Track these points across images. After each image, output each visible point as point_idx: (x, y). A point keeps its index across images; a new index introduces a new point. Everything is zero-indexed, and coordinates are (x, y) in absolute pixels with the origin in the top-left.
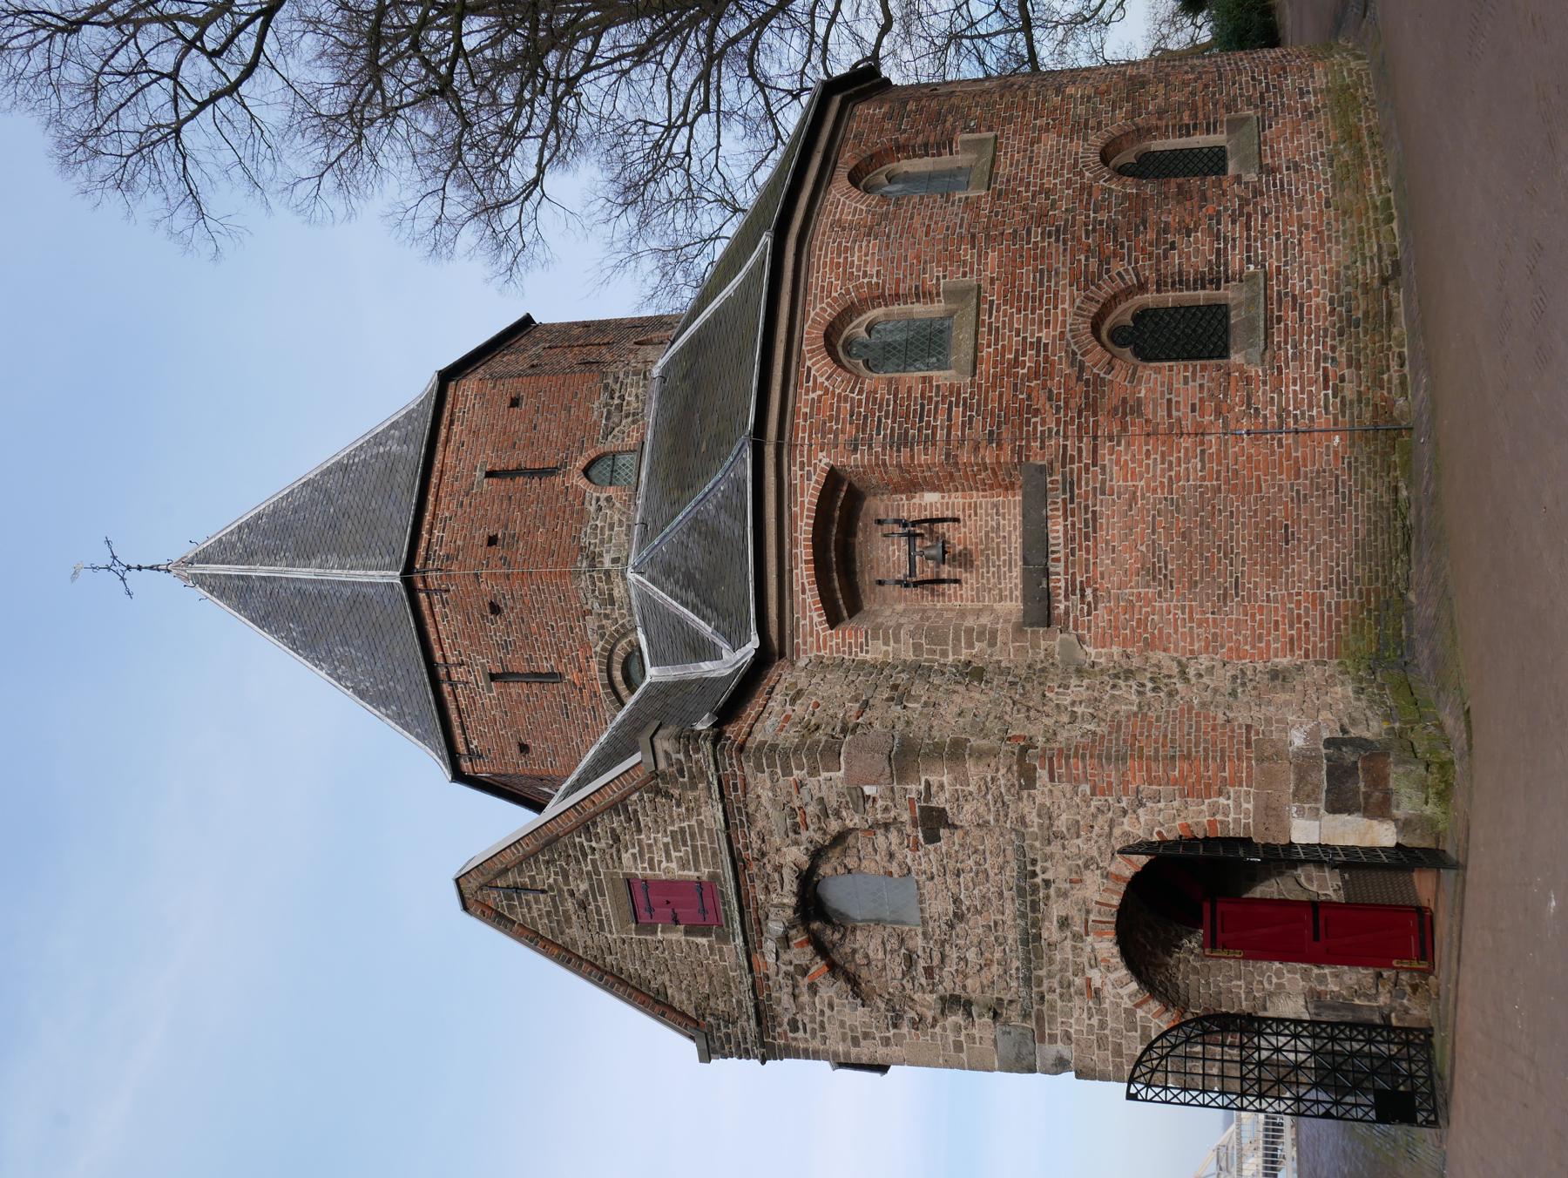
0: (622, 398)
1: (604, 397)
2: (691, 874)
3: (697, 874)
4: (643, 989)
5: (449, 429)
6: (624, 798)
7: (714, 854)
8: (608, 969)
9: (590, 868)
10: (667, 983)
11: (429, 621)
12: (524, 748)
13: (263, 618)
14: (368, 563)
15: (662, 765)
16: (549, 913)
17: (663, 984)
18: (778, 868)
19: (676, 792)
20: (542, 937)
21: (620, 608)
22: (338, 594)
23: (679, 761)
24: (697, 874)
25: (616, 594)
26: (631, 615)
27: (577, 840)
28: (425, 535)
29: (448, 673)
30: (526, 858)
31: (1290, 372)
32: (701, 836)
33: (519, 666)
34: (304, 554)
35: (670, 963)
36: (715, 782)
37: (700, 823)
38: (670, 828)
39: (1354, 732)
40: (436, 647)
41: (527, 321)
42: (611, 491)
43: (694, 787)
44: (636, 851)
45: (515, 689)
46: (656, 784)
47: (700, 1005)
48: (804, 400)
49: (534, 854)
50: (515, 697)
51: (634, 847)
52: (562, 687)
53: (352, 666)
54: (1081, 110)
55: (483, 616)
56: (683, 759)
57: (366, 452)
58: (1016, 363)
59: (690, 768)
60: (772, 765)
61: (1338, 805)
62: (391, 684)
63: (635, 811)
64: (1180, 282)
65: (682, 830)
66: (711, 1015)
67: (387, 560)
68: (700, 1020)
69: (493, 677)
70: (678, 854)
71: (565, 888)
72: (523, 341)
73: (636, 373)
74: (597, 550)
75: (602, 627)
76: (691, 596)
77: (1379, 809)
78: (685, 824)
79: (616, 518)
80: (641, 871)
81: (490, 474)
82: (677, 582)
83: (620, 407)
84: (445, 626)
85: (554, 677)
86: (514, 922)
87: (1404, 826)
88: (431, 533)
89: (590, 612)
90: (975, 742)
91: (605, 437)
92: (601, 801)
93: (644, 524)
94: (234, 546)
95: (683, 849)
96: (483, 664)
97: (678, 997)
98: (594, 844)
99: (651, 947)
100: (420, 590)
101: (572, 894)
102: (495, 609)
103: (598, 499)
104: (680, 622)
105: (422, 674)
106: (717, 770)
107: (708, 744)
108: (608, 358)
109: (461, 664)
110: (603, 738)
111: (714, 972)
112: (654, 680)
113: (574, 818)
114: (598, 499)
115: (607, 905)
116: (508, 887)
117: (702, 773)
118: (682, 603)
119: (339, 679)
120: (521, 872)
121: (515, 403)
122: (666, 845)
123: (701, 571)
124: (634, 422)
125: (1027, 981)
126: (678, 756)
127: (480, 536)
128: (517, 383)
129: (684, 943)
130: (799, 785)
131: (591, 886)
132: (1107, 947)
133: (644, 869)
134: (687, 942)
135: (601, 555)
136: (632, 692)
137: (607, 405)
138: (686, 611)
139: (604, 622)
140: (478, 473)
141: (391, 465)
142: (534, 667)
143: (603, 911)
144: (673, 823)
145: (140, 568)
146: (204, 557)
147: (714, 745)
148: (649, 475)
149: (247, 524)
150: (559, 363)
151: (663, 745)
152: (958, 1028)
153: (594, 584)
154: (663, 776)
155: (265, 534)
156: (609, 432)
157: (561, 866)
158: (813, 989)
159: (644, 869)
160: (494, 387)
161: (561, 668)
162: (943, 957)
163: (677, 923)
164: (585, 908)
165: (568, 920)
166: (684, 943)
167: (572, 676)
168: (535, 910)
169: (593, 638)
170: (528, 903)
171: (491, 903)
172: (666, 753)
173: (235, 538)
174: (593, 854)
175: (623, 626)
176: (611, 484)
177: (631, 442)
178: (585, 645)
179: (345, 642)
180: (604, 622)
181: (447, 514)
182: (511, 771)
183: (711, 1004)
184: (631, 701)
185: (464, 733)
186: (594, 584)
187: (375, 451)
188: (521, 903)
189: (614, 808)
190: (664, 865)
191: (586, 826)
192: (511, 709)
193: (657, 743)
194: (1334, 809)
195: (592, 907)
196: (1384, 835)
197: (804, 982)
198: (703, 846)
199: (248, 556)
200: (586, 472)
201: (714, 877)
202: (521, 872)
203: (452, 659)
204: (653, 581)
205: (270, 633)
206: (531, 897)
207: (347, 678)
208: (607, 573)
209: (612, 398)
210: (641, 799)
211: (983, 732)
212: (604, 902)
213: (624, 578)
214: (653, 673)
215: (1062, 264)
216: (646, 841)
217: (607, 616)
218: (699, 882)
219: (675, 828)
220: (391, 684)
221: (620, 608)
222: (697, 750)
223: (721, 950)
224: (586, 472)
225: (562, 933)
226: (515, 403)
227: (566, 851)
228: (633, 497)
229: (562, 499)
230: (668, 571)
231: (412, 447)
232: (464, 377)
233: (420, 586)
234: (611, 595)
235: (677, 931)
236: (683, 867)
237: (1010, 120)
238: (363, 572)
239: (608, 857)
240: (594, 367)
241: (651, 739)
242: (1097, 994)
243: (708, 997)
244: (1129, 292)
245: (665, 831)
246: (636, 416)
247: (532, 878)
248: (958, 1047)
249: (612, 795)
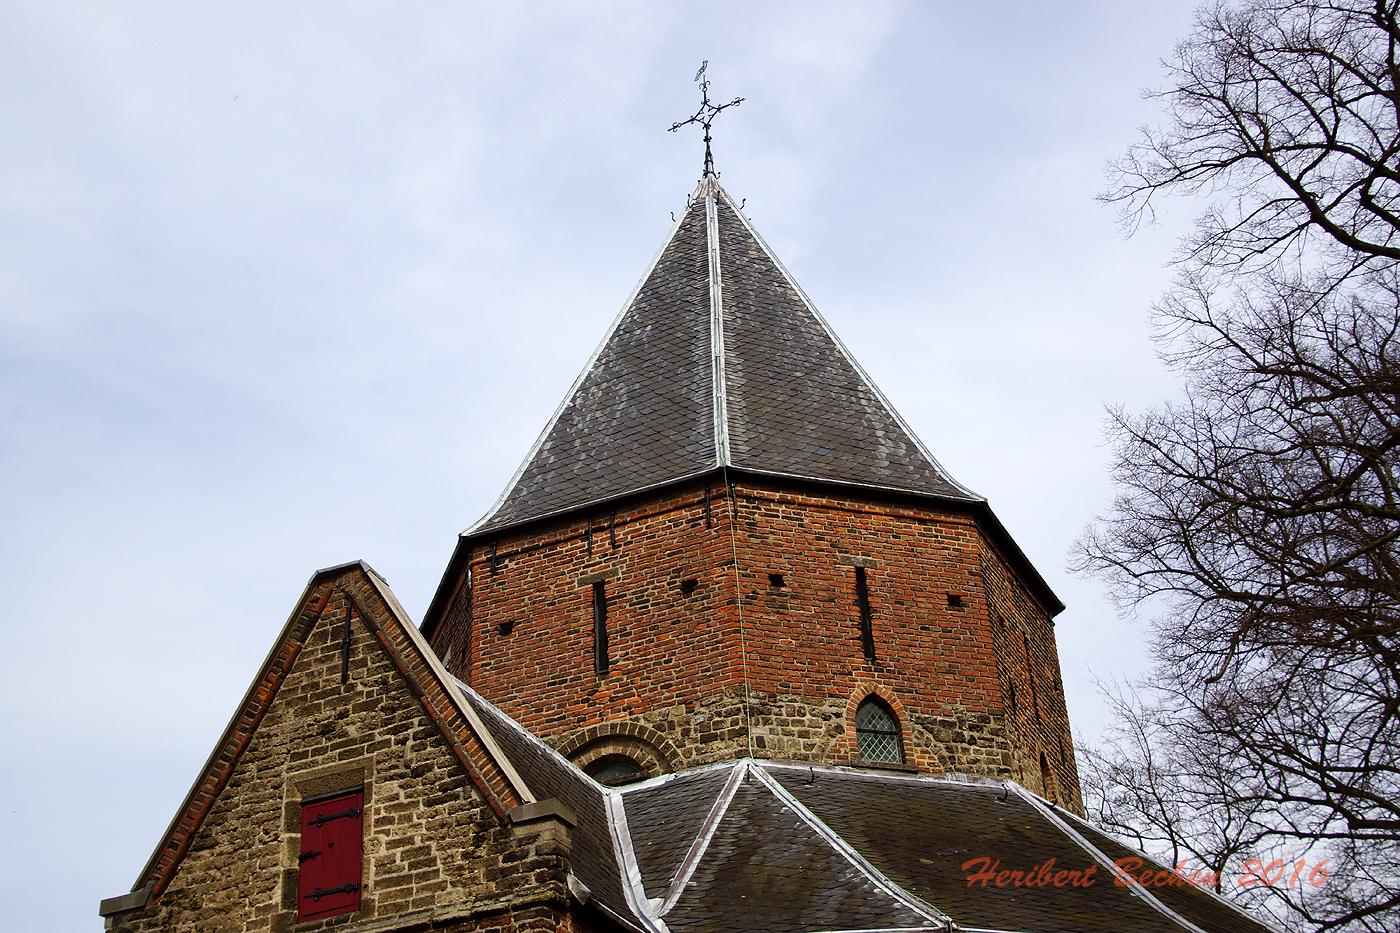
0: (972, 741)
1: (971, 718)
2: (371, 876)
3: (371, 884)
4: (210, 816)
5: (913, 519)
6: (472, 782)
7: (399, 907)
8: (238, 768)
9: (378, 738)
10: (217, 849)
12: (506, 628)
13: (654, 291)
14: (739, 423)
15: (520, 832)
16: (316, 685)
17: (217, 844)
19: (483, 852)
20: (283, 677)
21: (697, 749)
22: (694, 387)
23: (526, 854)
24: (371, 884)
25: (717, 744)
26: (690, 766)
27: (416, 721)
28: (777, 496)
29: (602, 529)
30: (388, 654)
32: (423, 889)
33: (615, 619)
34: (742, 342)
35: (247, 852)
36: (499, 906)
37: (441, 886)
38: (433, 844)
41: (1056, 607)
42: (851, 732)
43: (491, 876)
44: (403, 800)
45: (585, 615)
46: (494, 824)
47: (185, 896)
49: (395, 665)
50: (574, 614)
51: (407, 797)
52: (589, 674)
53: (602, 405)
55: (678, 571)
56: (528, 860)
57: (876, 414)
59: (515, 869)
62: (583, 456)
63: (456, 797)
65: (435, 859)
66: (171, 914)
67: (744, 448)
68: (163, 898)
69: (599, 587)
70: (398, 856)
71: (350, 707)
72: (1030, 604)
73: (1005, 757)
74: (773, 717)
75: (672, 725)
76: (727, 851)
78: (440, 865)
79: (816, 740)
80: (375, 808)
81: (860, 573)
82: (742, 829)
83: (959, 738)
84: (666, 526)
85: (603, 665)
86: (303, 641)
88: (781, 502)
89: (690, 710)
91: (919, 721)
92: (468, 750)
93: (814, 778)
94: (743, 253)
95: (406, 863)
96: (615, 572)
97: (197, 865)
98: (410, 743)
99: (267, 825)
100: (709, 491)
101: (343, 715)
102: (689, 587)
103: (838, 715)
104: (691, 833)
105: (599, 496)
106: (516, 908)
107: (550, 893)
108: (1022, 719)
109: (614, 545)
110: (531, 737)
111: (233, 914)
112: (605, 799)
113: (446, 715)
114: (838, 715)
115: (329, 763)
116: (351, 632)
117: (511, 887)
118: (715, 837)
119: (583, 388)
120: (370, 648)
121: (955, 601)
122: (410, 840)
123: (762, 863)
124: (942, 758)
126: (532, 853)
127: (782, 564)
128: (979, 602)
129: (274, 870)
131: (354, 741)
133: (378, 811)
134: (276, 875)
135: (766, 722)
136: (586, 770)
137: (962, 721)
138: (706, 843)
139: (678, 729)
140: (860, 557)
141: (862, 446)
142: (614, 638)
143: (319, 758)
144: (441, 848)
145: (707, 139)
146: (727, 218)
147: (551, 902)
148: (875, 784)
149: (772, 269)
150: (1009, 654)
151: (547, 832)
153: (729, 714)
154: (505, 833)
156: (929, 726)
157: (379, 701)
159: (378, 811)
160: (971, 573)
161: (614, 675)
163: (302, 859)
164: (323, 733)
165: (306, 712)
166: (274, 870)
168: (320, 667)
169: (656, 715)
170: (330, 658)
171: (329, 609)
172: (537, 836)
173: (753, 254)
174: (397, 742)
175: (675, 754)
176: (858, 731)
177: (916, 756)
178: (647, 705)
179: (632, 396)
180: (678, 729)
181: (806, 521)
182: (476, 612)
183: (187, 913)
184: (574, 768)
185: (524, 551)
186: (729, 714)
187: (876, 425)
188: (328, 649)
189: (460, 767)
190: (383, 838)
191: (435, 732)
192: (558, 610)
193: (548, 825)
195: (324, 743)
198: (409, 892)
199: (732, 272)
200: (872, 699)
201: (366, 908)
202: (370, 648)
203: (620, 533)
204: (741, 793)
205: (637, 302)
206: (338, 661)
207: (585, 399)
208: (744, 732)
209: (971, 728)
210: (472, 805)
212: (331, 758)
214: (614, 798)
216: (415, 813)
217: (686, 733)
218: (358, 888)
219: (434, 852)
220: (583, 456)
221: (697, 749)
222: (541, 879)
223: (264, 922)
224: (872, 699)
225: (288, 704)
226: (955, 601)
227: (400, 707)
228: (843, 761)
229: (837, 667)
230: (753, 815)
231: (887, 472)
232: (980, 534)
233: (714, 492)
234: (714, 738)
235: (291, 860)
236: (380, 865)
238: (725, 418)
239: (393, 762)
240: (1008, 702)
241: (554, 817)
243: (195, 907)
245: (430, 839)
246: (950, 763)
247: (363, 663)
249: (478, 766)
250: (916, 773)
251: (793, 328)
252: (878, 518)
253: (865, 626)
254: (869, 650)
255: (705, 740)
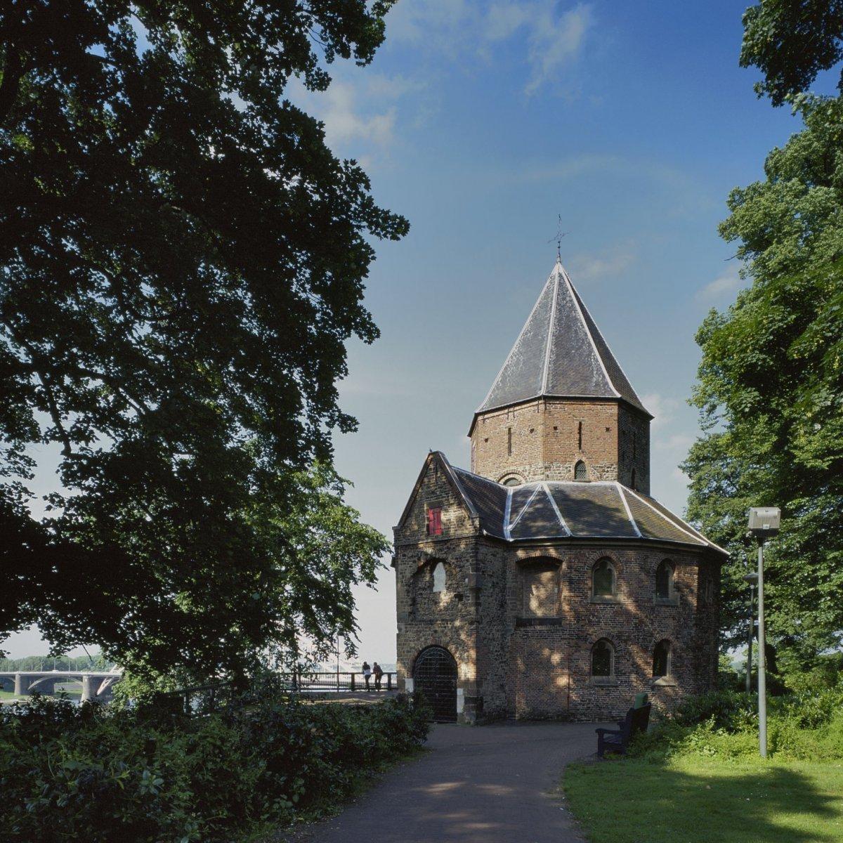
0: (608, 472)
1: (608, 465)
11: (528, 405)
18: (446, 553)
31: (586, 691)
39: (485, 704)
40: (520, 407)
42: (573, 471)
45: (506, 437)
48: (586, 552)
54: (685, 632)
58: (594, 616)
60: (473, 553)
61: (467, 700)
64: (617, 663)
67: (550, 385)
69: (510, 429)
77: (465, 709)
81: (580, 424)
83: (604, 471)
84: (527, 410)
85: (510, 452)
87: (462, 714)
90: (481, 609)
94: (564, 299)
102: (532, 431)
121: (608, 429)
125: (420, 621)
127: (557, 423)
130: (467, 561)
132: (429, 642)
148: (577, 487)
152: (407, 602)
155: (568, 316)
158: (414, 562)
162: (425, 598)
167: (511, 459)
177: (592, 478)
194: (466, 698)
196: (460, 708)
197: (416, 559)
200: (580, 462)
211: (483, 610)
213: (542, 480)
215: (625, 629)
226: (608, 429)
237: (684, 609)
242: (418, 640)
244: (615, 648)
248: (402, 602)
250: (590, 482)
251: (576, 331)
252: (587, 406)
253: (580, 440)
254: (580, 448)
255: (535, 475)
